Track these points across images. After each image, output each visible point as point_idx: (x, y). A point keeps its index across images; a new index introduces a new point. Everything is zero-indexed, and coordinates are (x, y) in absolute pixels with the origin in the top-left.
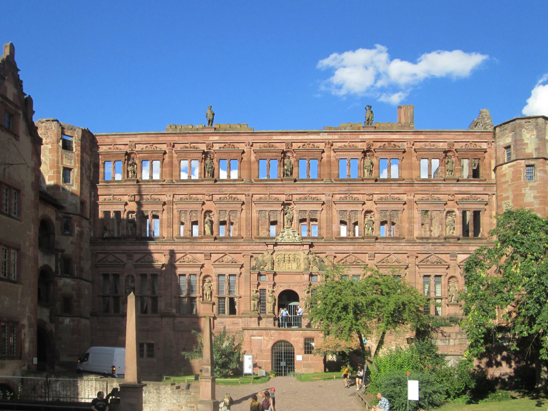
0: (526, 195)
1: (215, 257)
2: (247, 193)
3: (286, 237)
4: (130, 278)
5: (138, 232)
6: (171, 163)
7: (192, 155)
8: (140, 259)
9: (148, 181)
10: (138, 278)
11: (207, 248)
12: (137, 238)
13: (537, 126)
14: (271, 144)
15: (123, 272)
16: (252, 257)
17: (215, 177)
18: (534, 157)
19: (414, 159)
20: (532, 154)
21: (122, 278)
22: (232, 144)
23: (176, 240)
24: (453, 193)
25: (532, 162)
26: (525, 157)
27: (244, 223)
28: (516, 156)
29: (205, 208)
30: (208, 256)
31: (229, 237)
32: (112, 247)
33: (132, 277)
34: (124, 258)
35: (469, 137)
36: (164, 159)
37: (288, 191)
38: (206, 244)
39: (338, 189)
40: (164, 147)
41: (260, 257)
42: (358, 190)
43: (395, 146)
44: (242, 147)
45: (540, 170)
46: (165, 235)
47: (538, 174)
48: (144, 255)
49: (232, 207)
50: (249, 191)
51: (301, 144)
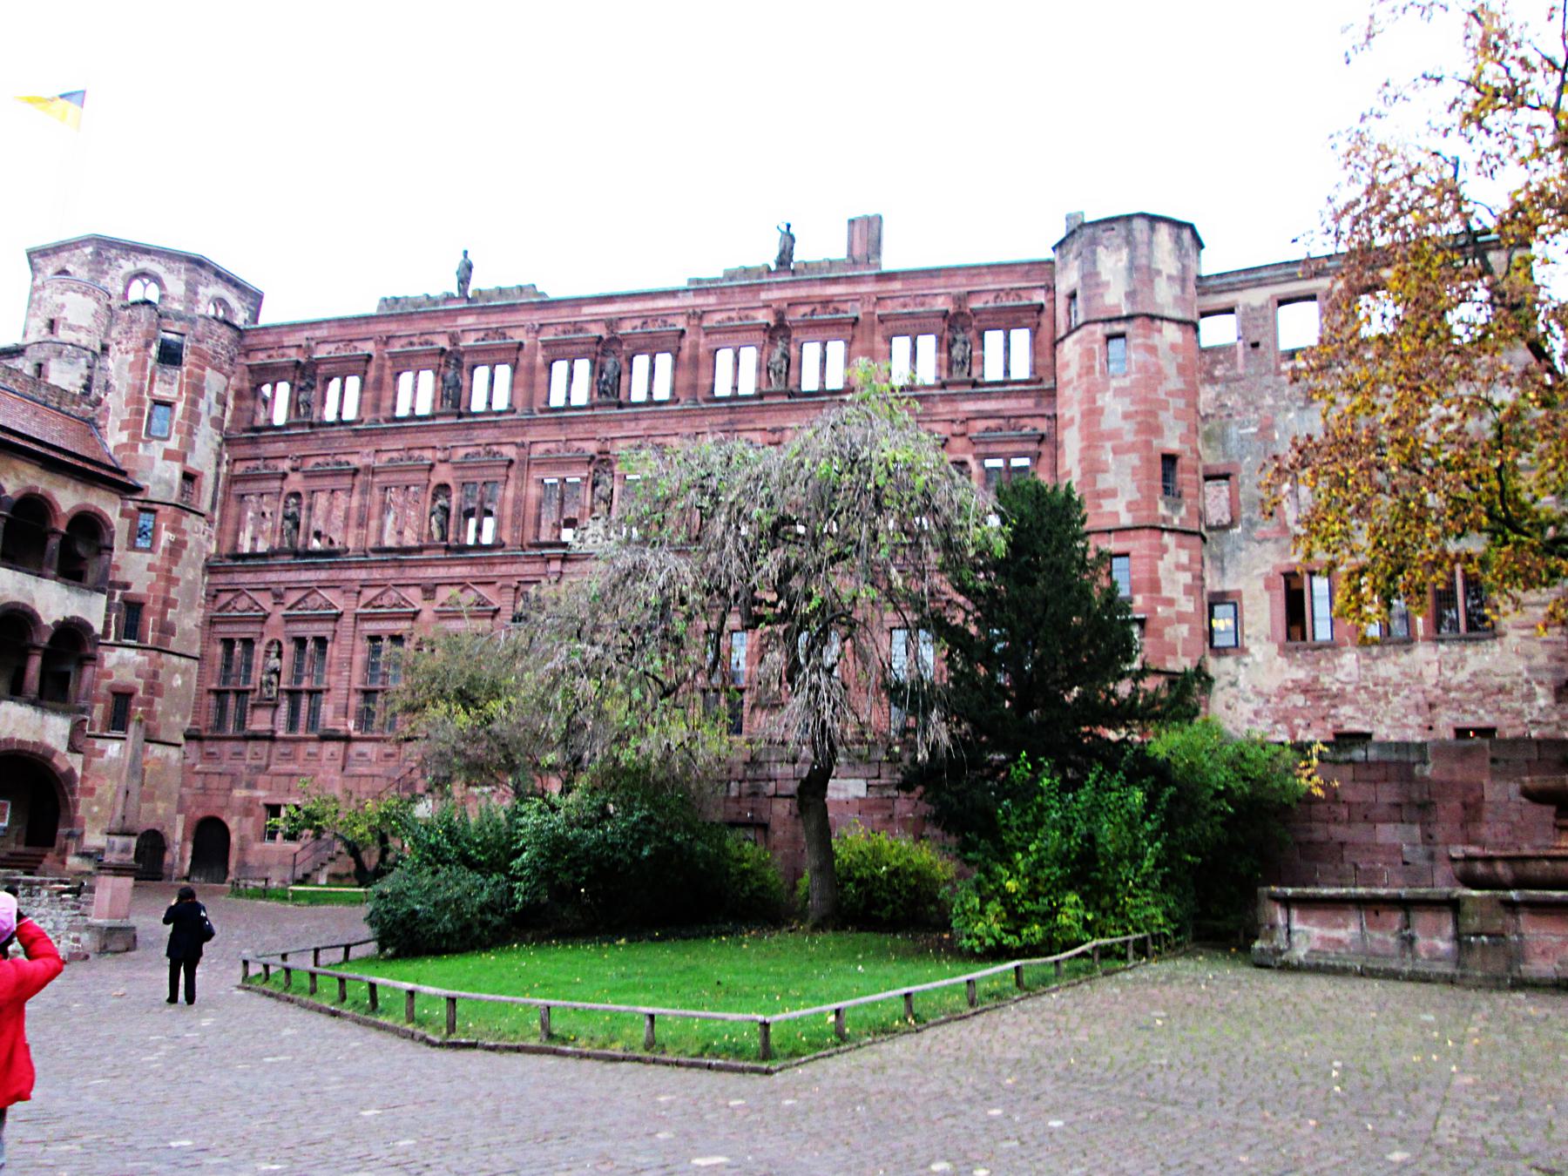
0: (1106, 411)
1: (443, 594)
2: (519, 440)
3: (590, 541)
4: (275, 648)
5: (301, 538)
6: (379, 383)
7: (420, 361)
8: (298, 602)
9: (332, 424)
10: (289, 648)
11: (430, 572)
12: (297, 554)
13: (1129, 241)
14: (578, 327)
15: (262, 634)
16: (517, 589)
17: (462, 409)
18: (1124, 313)
19: (878, 339)
20: (1118, 306)
21: (260, 648)
22: (500, 332)
23: (373, 557)
24: (961, 417)
25: (1118, 328)
26: (1102, 317)
27: (508, 510)
28: (1087, 313)
29: (436, 479)
30: (429, 591)
31: (478, 546)
32: (248, 578)
33: (280, 644)
34: (266, 602)
35: (1003, 278)
36: (366, 373)
37: (603, 432)
38: (427, 563)
39: (708, 420)
40: (369, 348)
41: (532, 589)
42: (751, 422)
43: (837, 311)
44: (519, 336)
45: (1137, 347)
46: (351, 545)
47: (1133, 356)
48: (303, 593)
49: (489, 474)
50: (524, 434)
51: (638, 322)
